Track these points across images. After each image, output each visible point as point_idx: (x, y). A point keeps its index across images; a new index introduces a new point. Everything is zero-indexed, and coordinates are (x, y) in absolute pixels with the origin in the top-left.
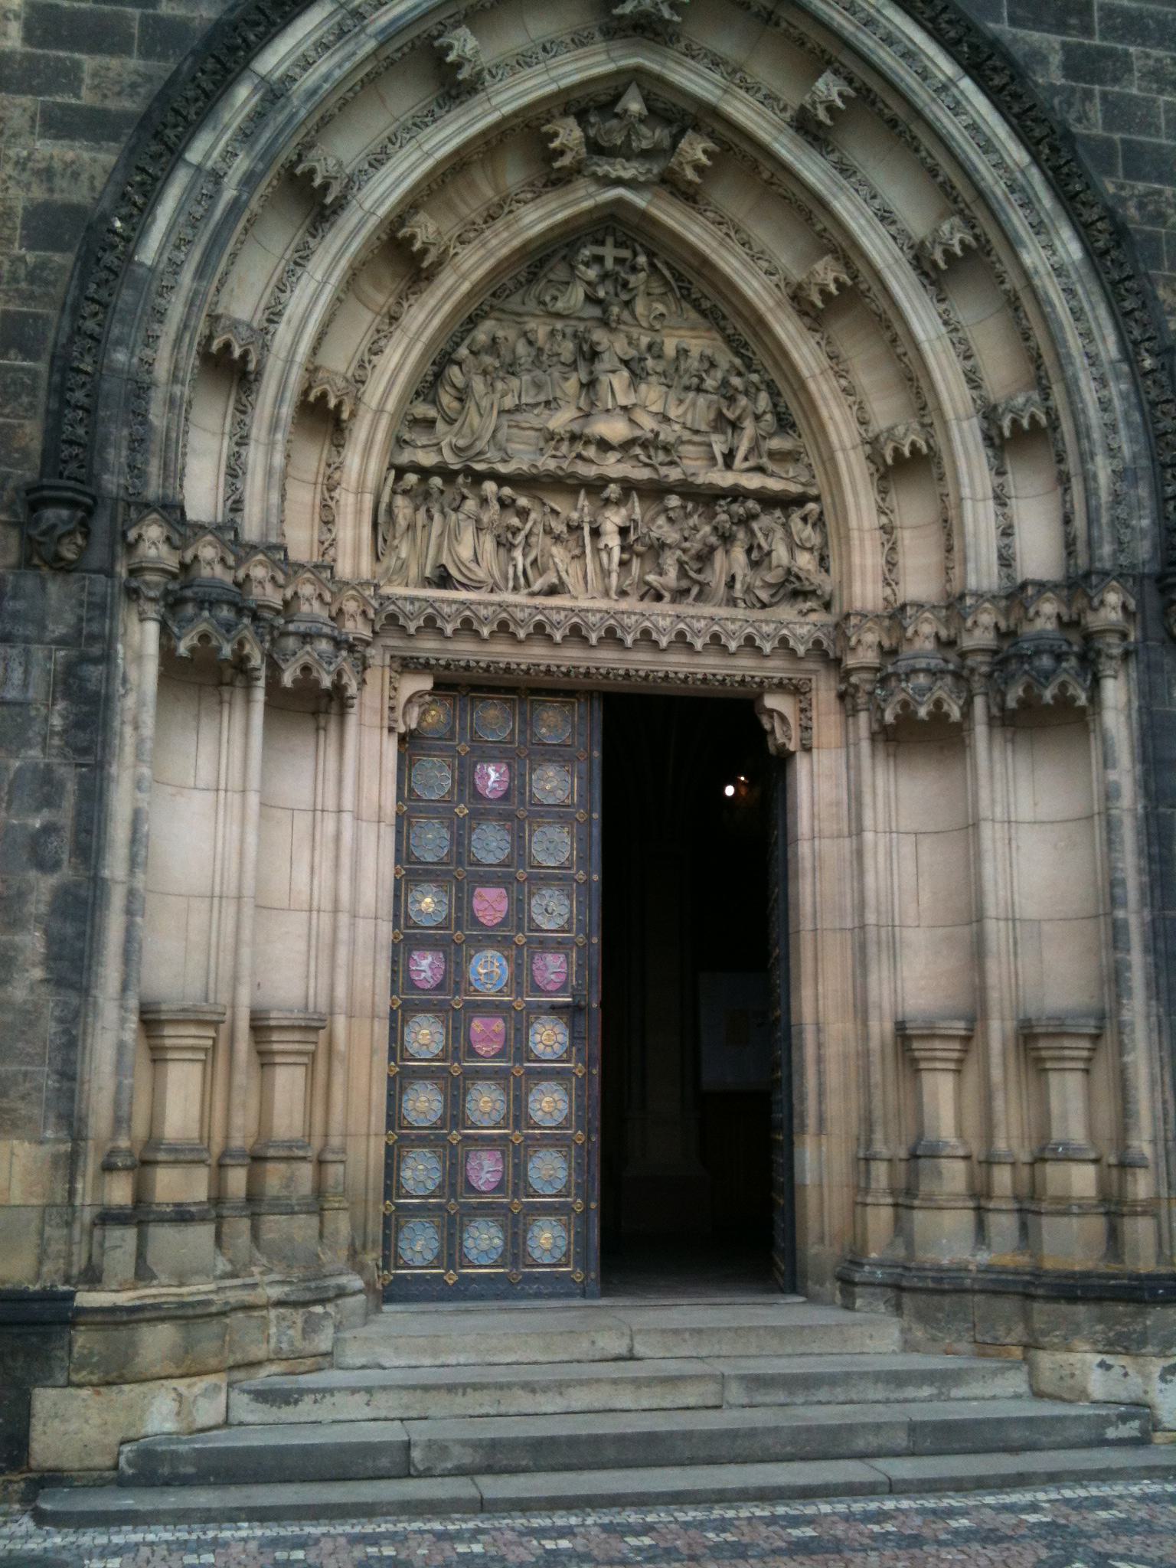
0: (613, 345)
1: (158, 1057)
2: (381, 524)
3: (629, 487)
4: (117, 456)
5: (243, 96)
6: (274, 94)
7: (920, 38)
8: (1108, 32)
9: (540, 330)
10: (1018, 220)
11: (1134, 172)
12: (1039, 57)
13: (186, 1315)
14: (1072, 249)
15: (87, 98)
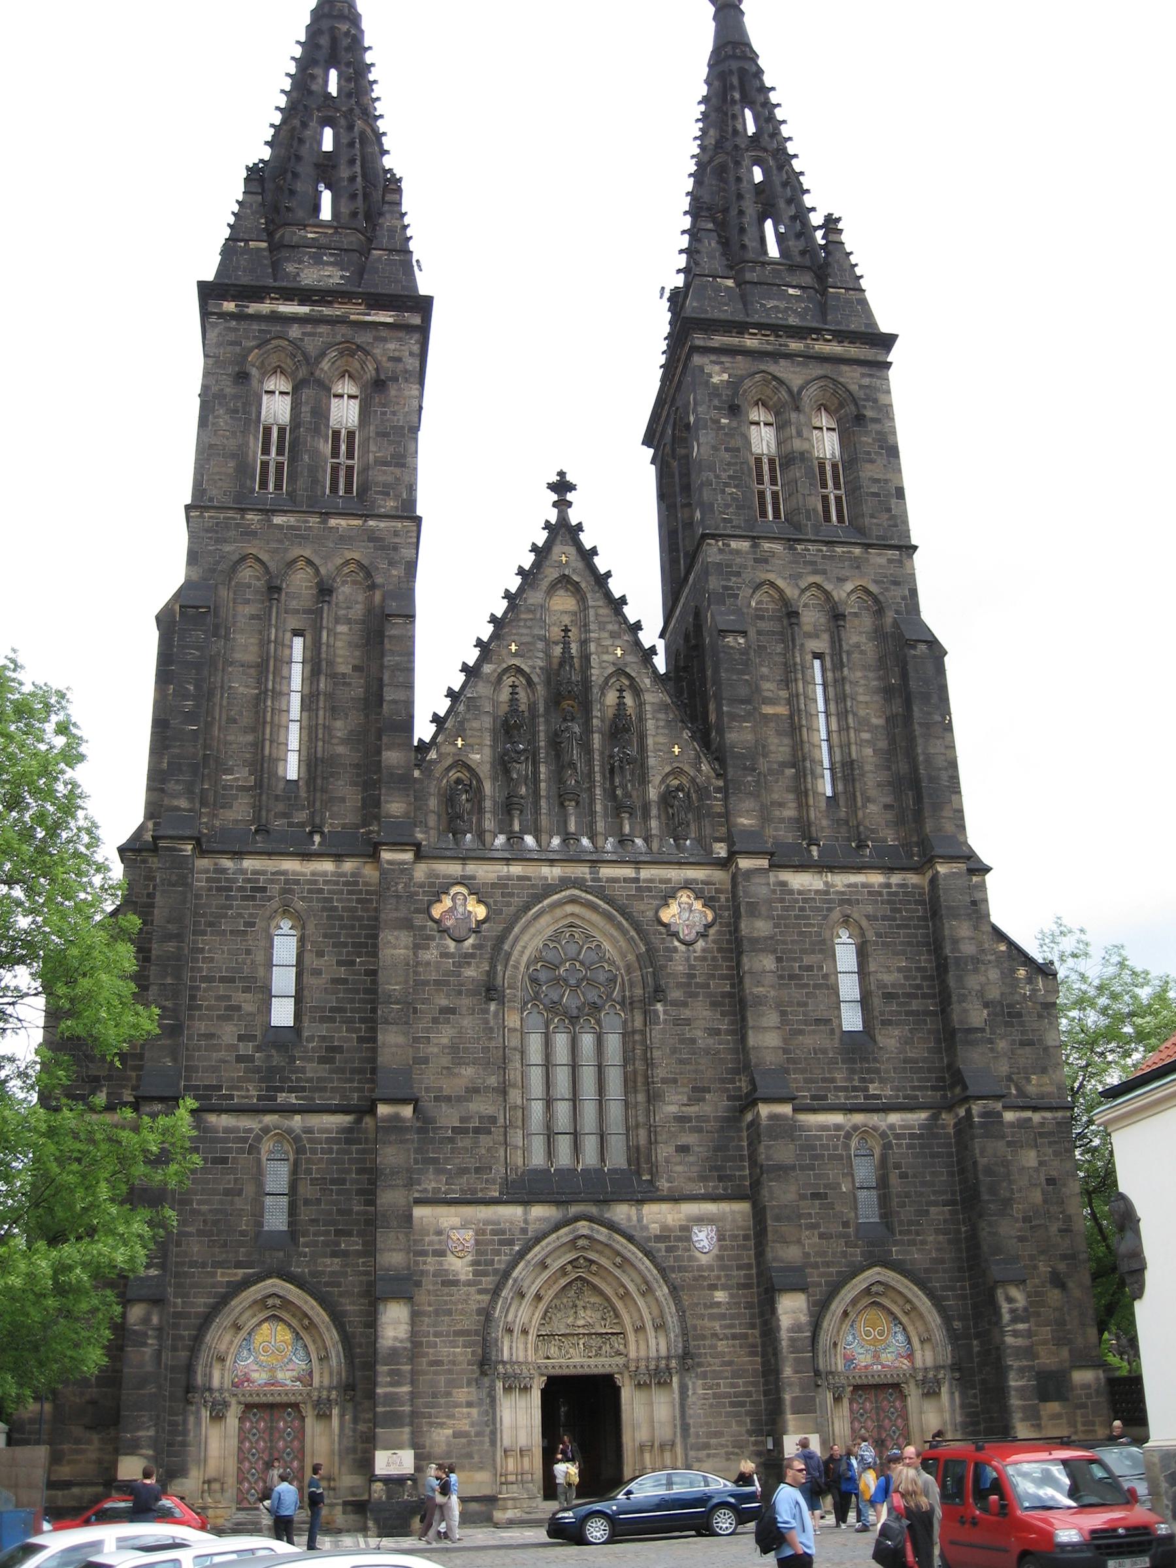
0: (580, 1303)
1: (506, 1456)
2: (536, 1349)
3: (584, 1334)
4: (494, 1353)
5: (511, 1281)
6: (515, 1281)
7: (635, 1250)
8: (675, 1241)
9: (565, 1301)
10: (655, 1285)
11: (680, 1272)
12: (659, 1250)
13: (513, 1499)
14: (666, 1290)
15: (484, 1286)
